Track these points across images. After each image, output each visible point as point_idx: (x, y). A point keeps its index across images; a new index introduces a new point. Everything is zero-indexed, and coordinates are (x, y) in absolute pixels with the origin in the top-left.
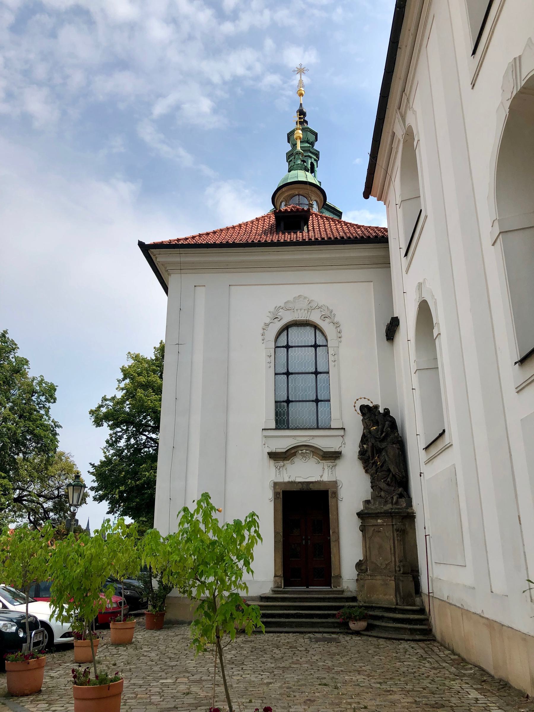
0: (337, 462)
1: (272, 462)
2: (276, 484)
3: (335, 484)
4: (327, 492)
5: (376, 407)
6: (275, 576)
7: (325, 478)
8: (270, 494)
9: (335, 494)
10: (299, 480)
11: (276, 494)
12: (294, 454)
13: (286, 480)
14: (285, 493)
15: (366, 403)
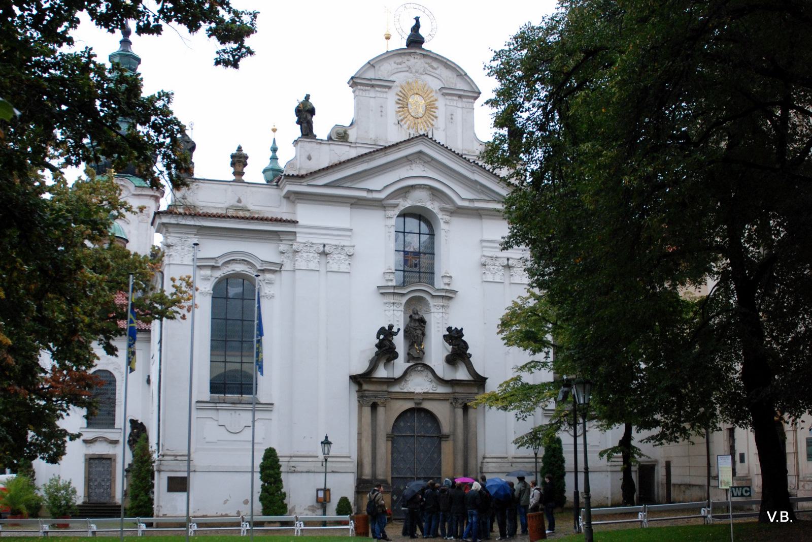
0: (117, 445)
1: (84, 444)
2: (86, 455)
3: (115, 455)
4: (110, 459)
5: (137, 421)
6: (84, 497)
7: (110, 453)
8: (83, 460)
9: (115, 460)
10: (97, 453)
11: (86, 460)
12: (96, 441)
13: (91, 453)
14: (90, 459)
15: (133, 418)
